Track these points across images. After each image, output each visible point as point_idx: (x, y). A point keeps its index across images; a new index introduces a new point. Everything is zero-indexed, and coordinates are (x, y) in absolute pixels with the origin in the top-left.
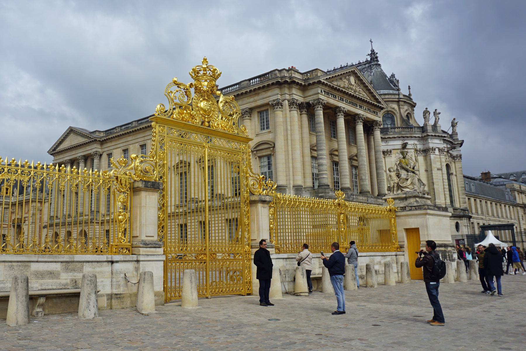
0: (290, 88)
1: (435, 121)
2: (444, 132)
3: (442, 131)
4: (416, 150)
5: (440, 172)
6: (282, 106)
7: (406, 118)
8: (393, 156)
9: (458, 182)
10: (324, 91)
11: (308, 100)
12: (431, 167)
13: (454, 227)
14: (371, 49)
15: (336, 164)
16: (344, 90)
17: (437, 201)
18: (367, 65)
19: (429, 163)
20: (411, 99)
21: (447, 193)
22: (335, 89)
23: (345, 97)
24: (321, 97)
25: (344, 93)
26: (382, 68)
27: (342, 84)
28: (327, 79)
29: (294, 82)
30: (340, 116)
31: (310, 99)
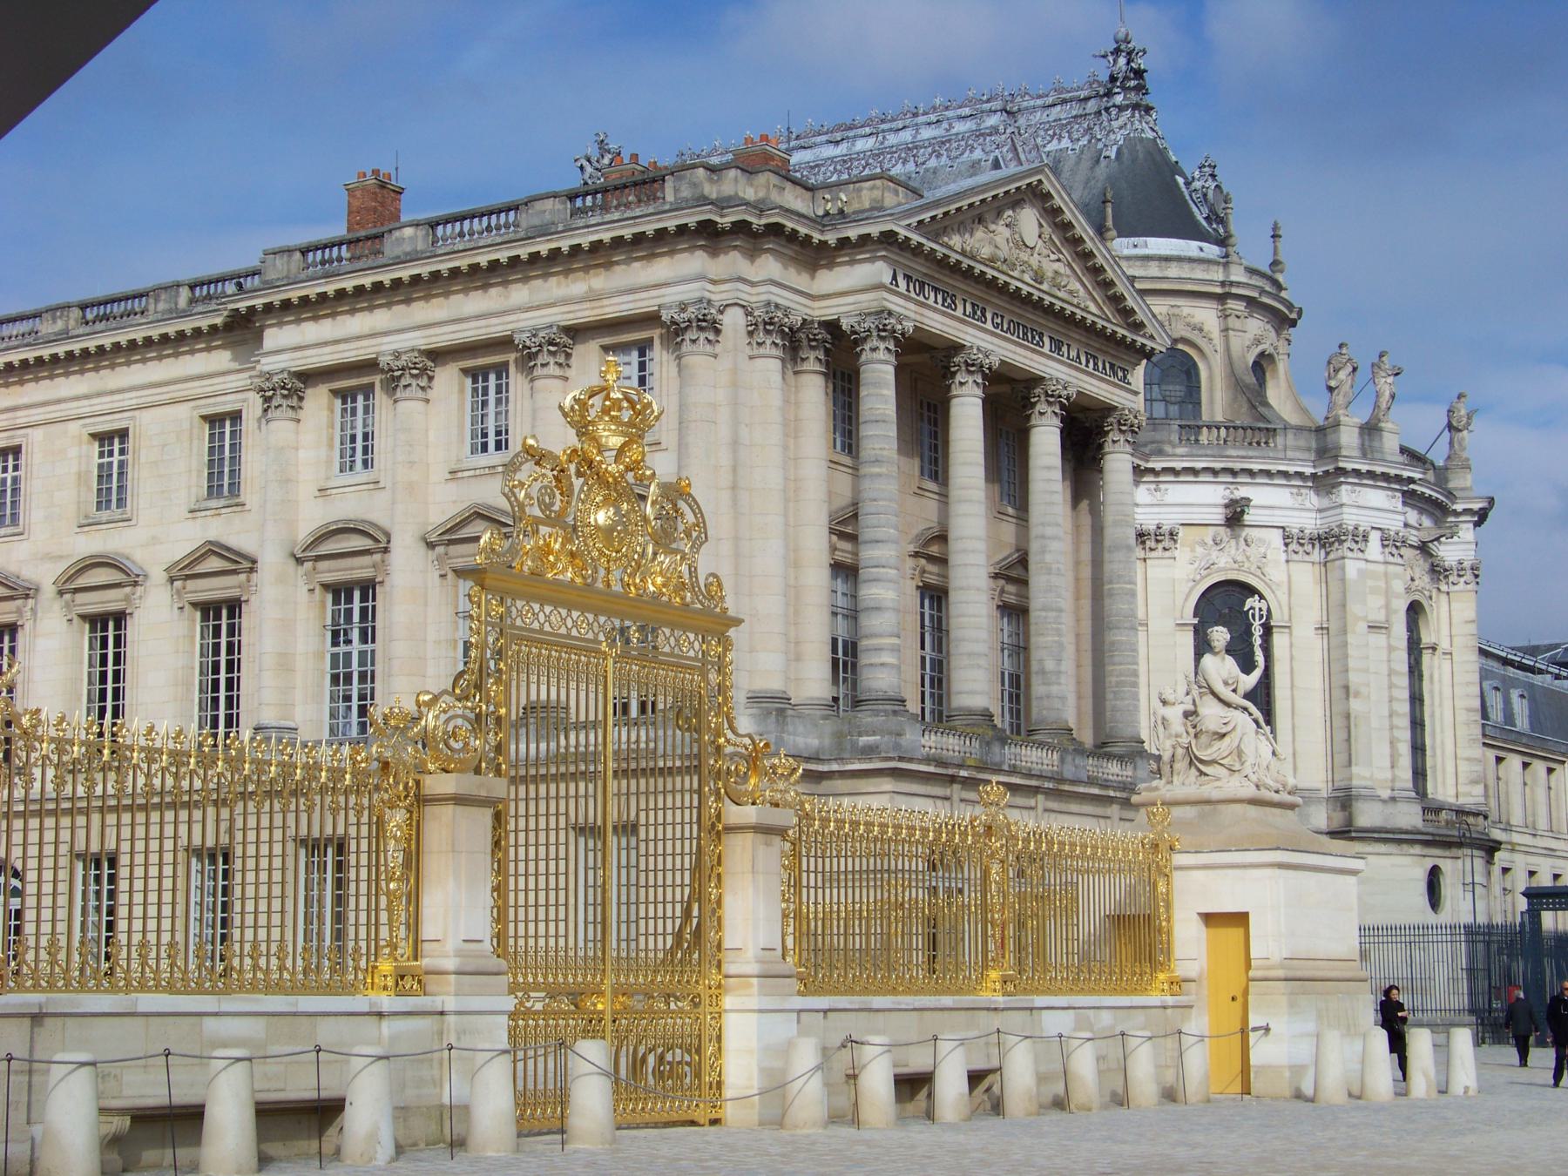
1: (1376, 406)
3: (1403, 450)
4: (1287, 538)
5: (1379, 639)
6: (718, 332)
7: (1251, 379)
8: (1182, 553)
9: (1454, 684)
10: (908, 278)
12: (1344, 618)
13: (1422, 887)
15: (935, 596)
16: (990, 273)
17: (1354, 769)
18: (1092, 106)
19: (1335, 596)
20: (1279, 287)
21: (1405, 735)
22: (955, 269)
24: (895, 304)
25: (992, 284)
27: (982, 245)
28: (920, 222)
31: (845, 311)
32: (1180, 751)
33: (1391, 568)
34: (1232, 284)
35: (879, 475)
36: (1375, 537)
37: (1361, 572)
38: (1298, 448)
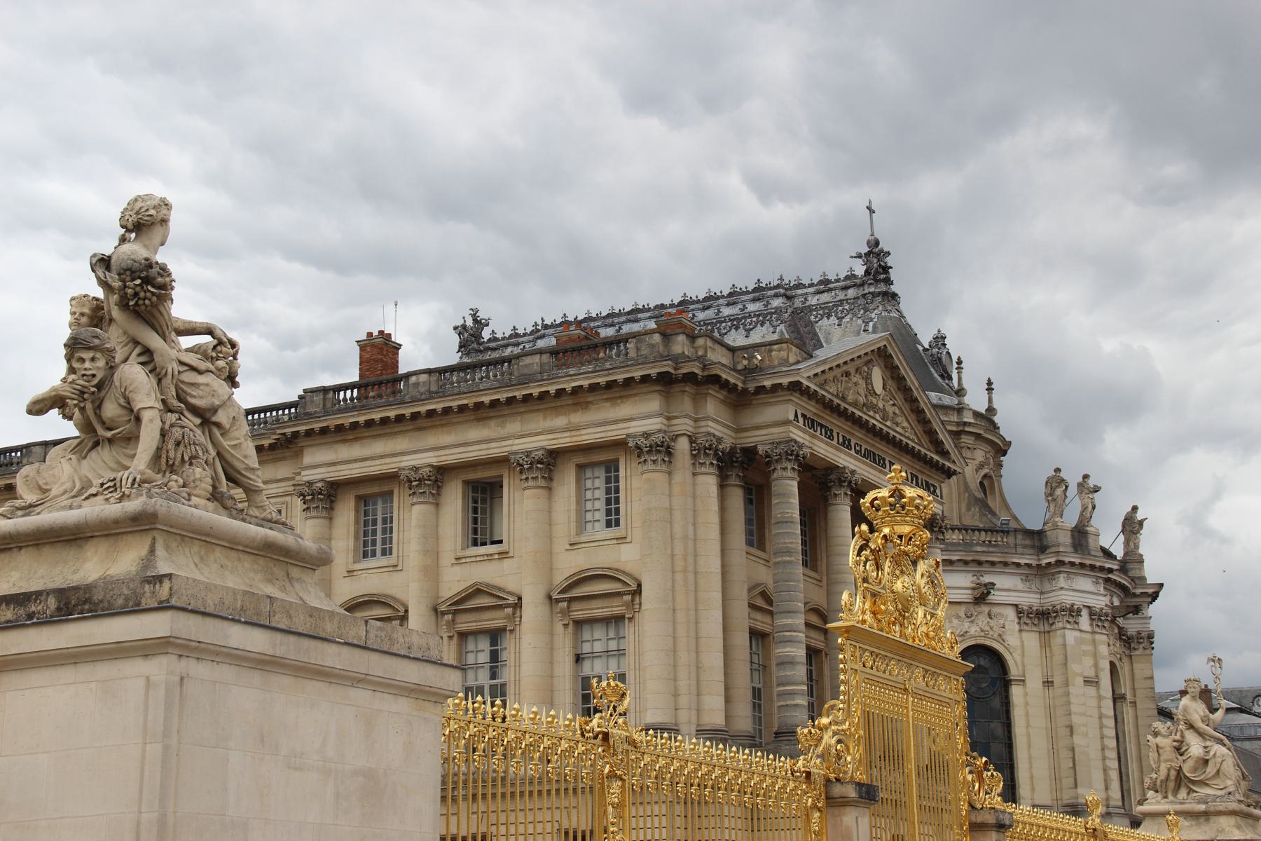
0: (697, 399)
2: (1107, 554)
5: (1091, 691)
6: (669, 454)
7: (980, 495)
10: (803, 415)
11: (749, 439)
14: (867, 237)
16: (858, 413)
18: (851, 293)
23: (857, 436)
26: (902, 307)
27: (855, 392)
28: (816, 375)
29: (715, 380)
30: (839, 500)
32: (1173, 773)
33: (1097, 637)
34: (965, 424)
35: (790, 562)
36: (1085, 613)
37: (1076, 638)
38: (1025, 546)
